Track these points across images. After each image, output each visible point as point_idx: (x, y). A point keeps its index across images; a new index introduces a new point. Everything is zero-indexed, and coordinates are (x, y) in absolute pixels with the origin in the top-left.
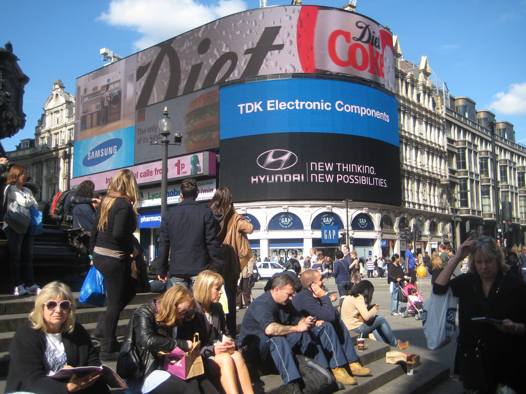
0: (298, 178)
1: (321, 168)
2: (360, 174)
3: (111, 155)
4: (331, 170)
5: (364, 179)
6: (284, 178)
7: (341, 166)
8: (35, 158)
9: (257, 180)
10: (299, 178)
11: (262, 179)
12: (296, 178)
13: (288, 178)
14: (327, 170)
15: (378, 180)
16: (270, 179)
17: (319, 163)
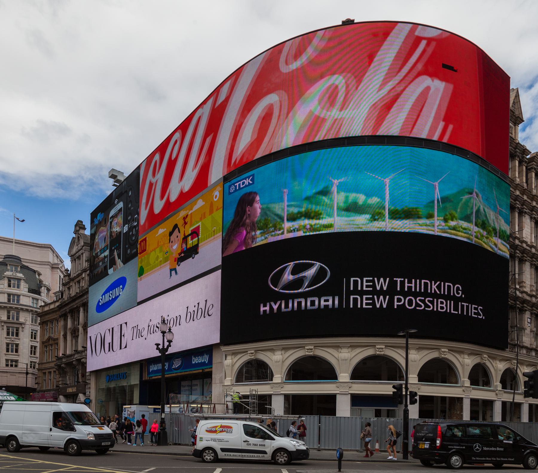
0: (328, 302)
1: (367, 286)
2: (435, 296)
3: (118, 297)
4: (385, 288)
5: (442, 303)
6: (306, 304)
7: (402, 283)
8: (62, 310)
9: (267, 308)
10: (330, 303)
11: (275, 307)
12: (326, 303)
13: (313, 303)
14: (378, 288)
15: (468, 307)
16: (287, 306)
17: (365, 279)
